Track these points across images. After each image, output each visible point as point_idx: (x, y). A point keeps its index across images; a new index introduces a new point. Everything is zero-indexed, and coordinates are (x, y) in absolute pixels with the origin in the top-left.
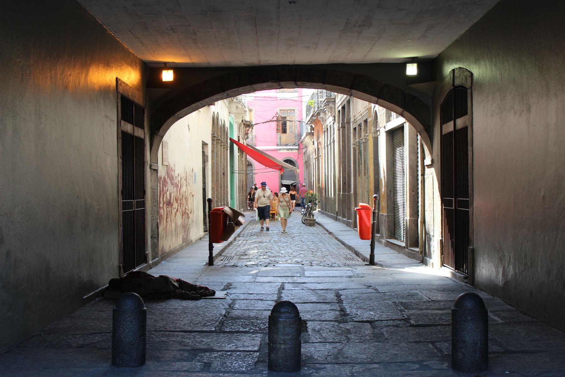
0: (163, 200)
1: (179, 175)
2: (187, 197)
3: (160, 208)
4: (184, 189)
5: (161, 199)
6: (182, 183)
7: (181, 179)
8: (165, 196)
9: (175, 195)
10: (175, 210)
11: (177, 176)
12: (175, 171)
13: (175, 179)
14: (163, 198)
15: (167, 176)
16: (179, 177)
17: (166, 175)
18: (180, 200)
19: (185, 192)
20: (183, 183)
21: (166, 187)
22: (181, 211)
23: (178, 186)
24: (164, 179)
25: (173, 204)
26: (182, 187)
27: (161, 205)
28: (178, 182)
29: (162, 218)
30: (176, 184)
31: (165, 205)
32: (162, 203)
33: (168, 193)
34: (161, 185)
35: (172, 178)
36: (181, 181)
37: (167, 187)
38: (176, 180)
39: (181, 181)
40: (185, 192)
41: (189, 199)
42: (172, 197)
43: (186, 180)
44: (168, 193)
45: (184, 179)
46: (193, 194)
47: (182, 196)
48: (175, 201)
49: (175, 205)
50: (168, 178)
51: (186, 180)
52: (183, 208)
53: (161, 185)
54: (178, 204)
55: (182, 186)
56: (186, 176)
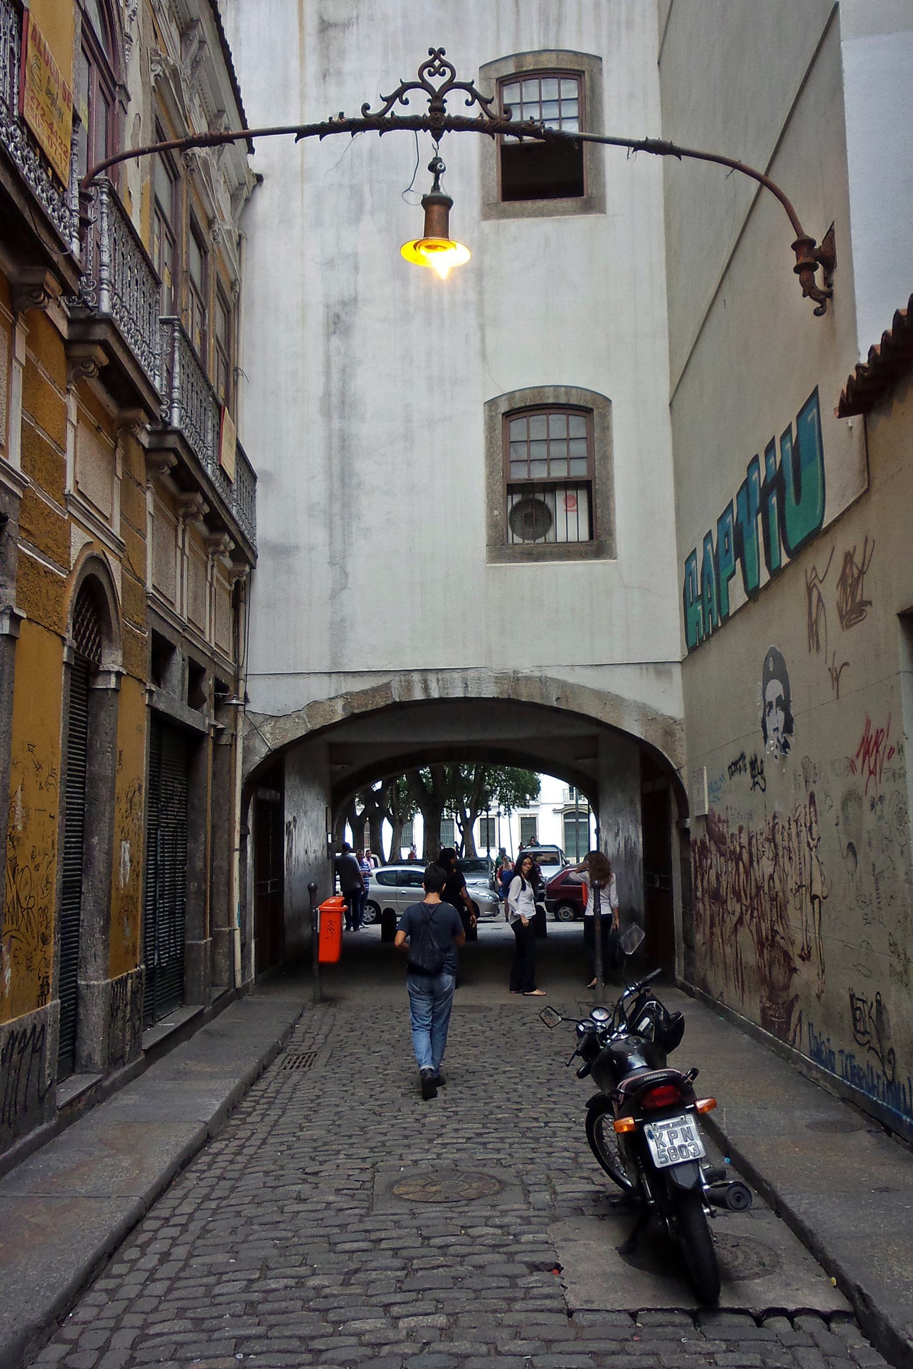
0: (702, 885)
1: (741, 829)
2: (781, 894)
3: (697, 898)
4: (766, 866)
5: (699, 882)
6: (754, 850)
7: (750, 839)
8: (706, 877)
9: (730, 880)
10: (735, 919)
11: (737, 833)
12: (728, 821)
13: (729, 840)
14: (702, 882)
15: (707, 837)
16: (744, 835)
17: (704, 836)
18: (751, 898)
19: (771, 877)
20: (758, 850)
21: (706, 859)
22: (753, 928)
23: (740, 858)
24: (703, 842)
25: (726, 901)
26: (755, 863)
27: (699, 894)
28: (741, 847)
29: (701, 918)
30: (734, 852)
31: (707, 895)
32: (700, 889)
33: (713, 873)
34: (697, 856)
35: (719, 840)
36: (750, 844)
37: (709, 861)
38: (732, 842)
39: (750, 844)
40: (771, 877)
41: (790, 907)
42: (724, 884)
43: (774, 839)
44: (713, 873)
45: (761, 839)
46: (817, 889)
47: (759, 888)
48: (730, 895)
49: (733, 906)
50: (710, 841)
51: (772, 840)
52: (763, 925)
53: (697, 856)
54: (744, 908)
55: (755, 859)
56: (774, 827)
